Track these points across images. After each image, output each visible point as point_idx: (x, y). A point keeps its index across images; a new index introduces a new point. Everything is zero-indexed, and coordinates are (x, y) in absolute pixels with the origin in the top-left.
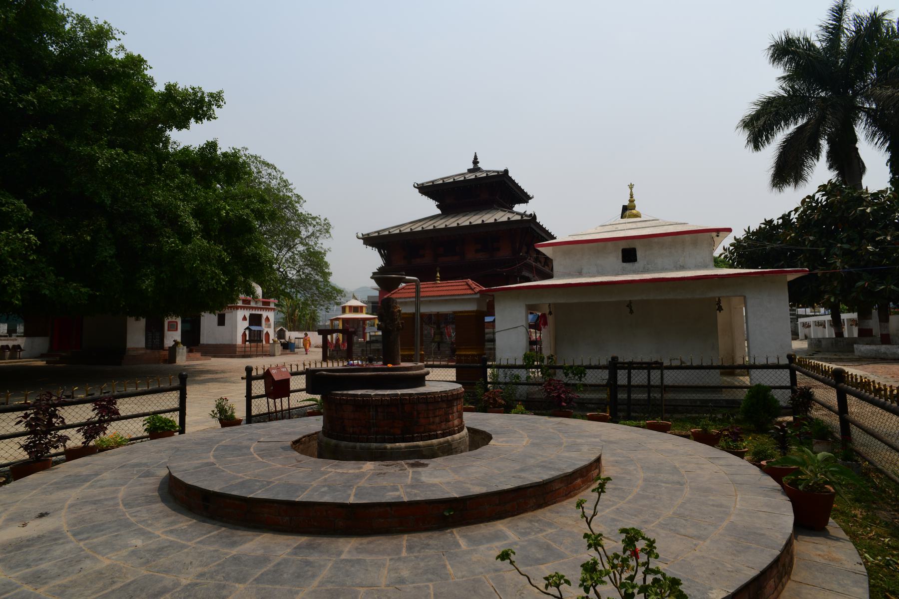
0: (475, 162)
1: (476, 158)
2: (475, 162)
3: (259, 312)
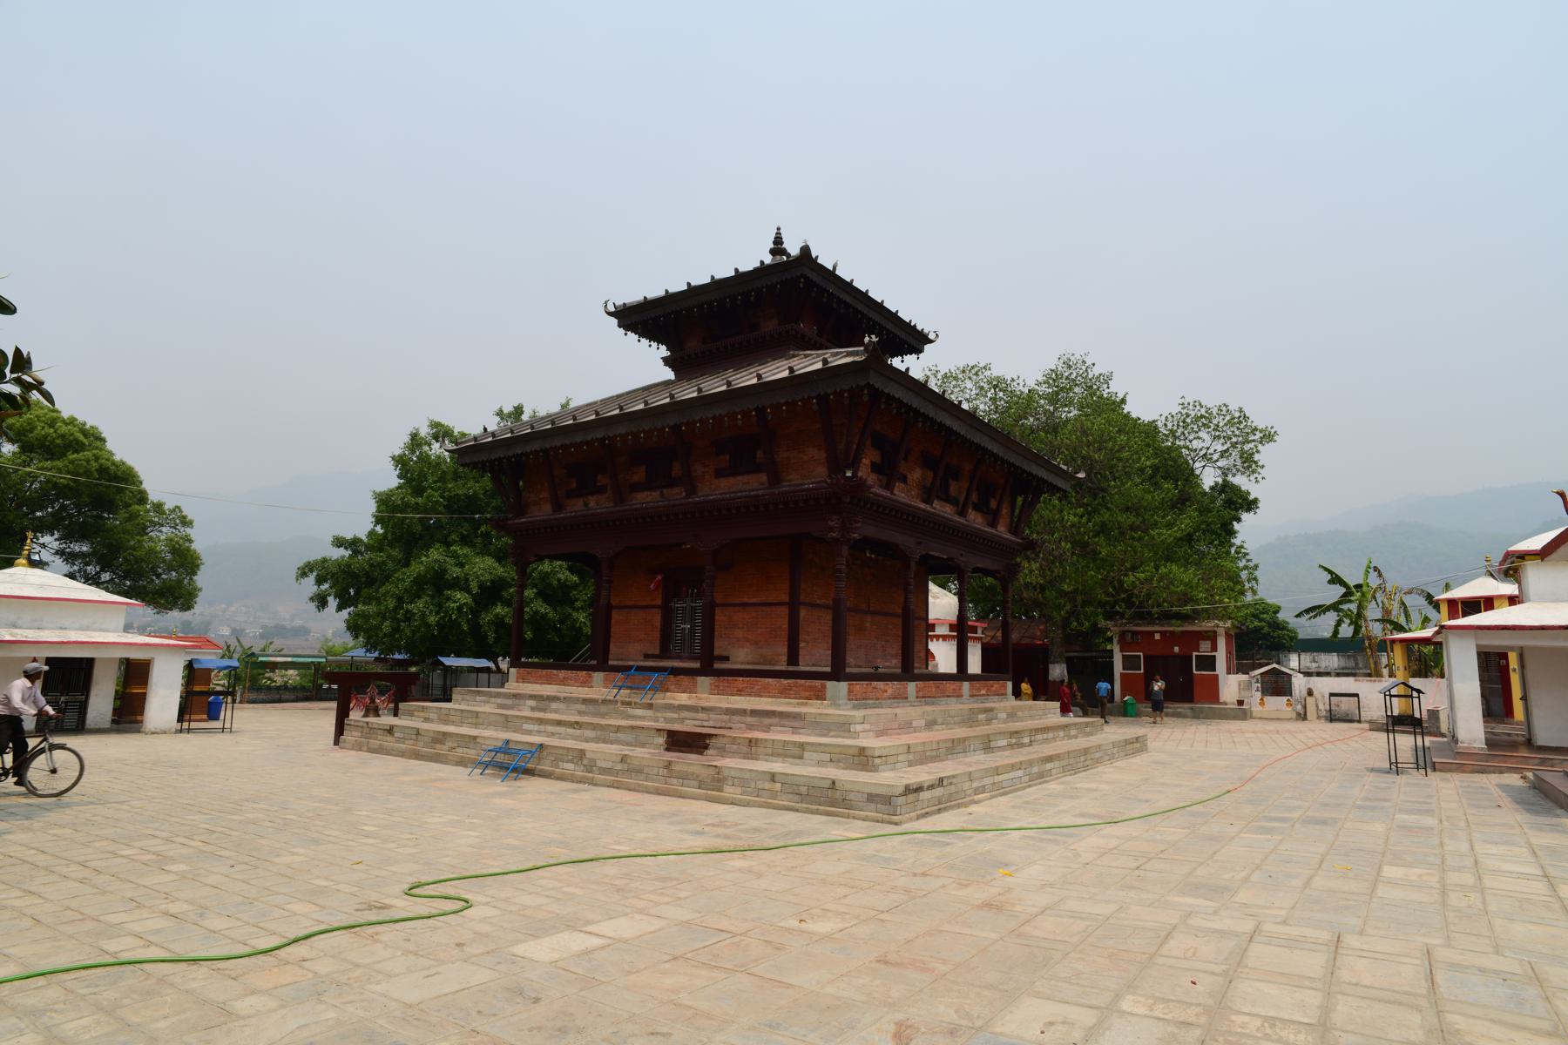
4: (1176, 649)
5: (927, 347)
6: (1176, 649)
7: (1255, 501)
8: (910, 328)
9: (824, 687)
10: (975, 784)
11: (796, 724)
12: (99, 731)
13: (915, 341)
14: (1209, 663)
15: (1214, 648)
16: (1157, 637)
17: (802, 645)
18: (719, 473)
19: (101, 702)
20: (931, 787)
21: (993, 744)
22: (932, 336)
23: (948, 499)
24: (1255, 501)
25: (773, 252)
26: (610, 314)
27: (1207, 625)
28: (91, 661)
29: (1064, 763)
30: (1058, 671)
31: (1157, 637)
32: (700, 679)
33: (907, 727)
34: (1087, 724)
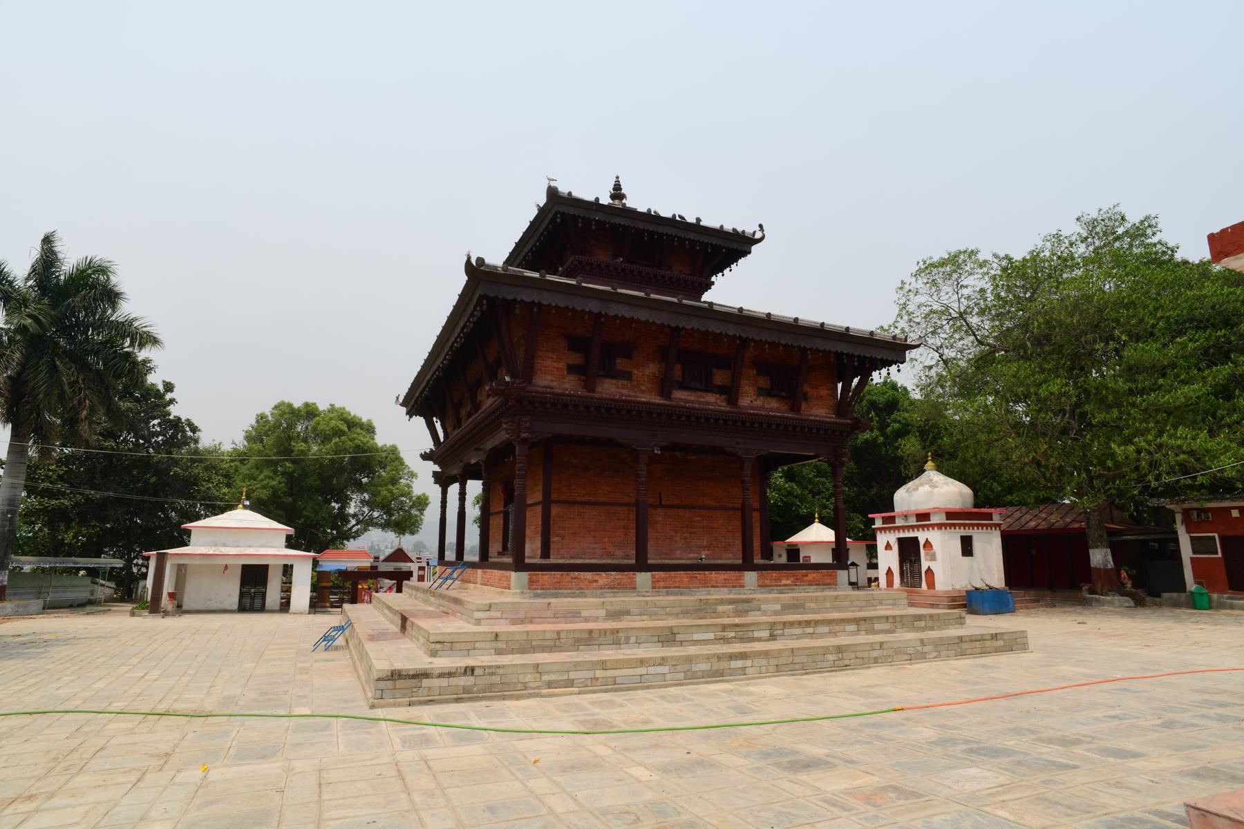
0: (617, 193)
1: (617, 187)
2: (617, 193)
3: (911, 534)
5: (754, 248)
8: (719, 233)
10: (546, 678)
12: (272, 611)
13: (730, 247)
16: (1235, 513)
19: (273, 594)
20: (441, 676)
21: (679, 637)
23: (709, 388)
25: (613, 197)
28: (266, 566)
29: (773, 662)
30: (1099, 557)
31: (1235, 513)
33: (575, 615)
34: (919, 618)
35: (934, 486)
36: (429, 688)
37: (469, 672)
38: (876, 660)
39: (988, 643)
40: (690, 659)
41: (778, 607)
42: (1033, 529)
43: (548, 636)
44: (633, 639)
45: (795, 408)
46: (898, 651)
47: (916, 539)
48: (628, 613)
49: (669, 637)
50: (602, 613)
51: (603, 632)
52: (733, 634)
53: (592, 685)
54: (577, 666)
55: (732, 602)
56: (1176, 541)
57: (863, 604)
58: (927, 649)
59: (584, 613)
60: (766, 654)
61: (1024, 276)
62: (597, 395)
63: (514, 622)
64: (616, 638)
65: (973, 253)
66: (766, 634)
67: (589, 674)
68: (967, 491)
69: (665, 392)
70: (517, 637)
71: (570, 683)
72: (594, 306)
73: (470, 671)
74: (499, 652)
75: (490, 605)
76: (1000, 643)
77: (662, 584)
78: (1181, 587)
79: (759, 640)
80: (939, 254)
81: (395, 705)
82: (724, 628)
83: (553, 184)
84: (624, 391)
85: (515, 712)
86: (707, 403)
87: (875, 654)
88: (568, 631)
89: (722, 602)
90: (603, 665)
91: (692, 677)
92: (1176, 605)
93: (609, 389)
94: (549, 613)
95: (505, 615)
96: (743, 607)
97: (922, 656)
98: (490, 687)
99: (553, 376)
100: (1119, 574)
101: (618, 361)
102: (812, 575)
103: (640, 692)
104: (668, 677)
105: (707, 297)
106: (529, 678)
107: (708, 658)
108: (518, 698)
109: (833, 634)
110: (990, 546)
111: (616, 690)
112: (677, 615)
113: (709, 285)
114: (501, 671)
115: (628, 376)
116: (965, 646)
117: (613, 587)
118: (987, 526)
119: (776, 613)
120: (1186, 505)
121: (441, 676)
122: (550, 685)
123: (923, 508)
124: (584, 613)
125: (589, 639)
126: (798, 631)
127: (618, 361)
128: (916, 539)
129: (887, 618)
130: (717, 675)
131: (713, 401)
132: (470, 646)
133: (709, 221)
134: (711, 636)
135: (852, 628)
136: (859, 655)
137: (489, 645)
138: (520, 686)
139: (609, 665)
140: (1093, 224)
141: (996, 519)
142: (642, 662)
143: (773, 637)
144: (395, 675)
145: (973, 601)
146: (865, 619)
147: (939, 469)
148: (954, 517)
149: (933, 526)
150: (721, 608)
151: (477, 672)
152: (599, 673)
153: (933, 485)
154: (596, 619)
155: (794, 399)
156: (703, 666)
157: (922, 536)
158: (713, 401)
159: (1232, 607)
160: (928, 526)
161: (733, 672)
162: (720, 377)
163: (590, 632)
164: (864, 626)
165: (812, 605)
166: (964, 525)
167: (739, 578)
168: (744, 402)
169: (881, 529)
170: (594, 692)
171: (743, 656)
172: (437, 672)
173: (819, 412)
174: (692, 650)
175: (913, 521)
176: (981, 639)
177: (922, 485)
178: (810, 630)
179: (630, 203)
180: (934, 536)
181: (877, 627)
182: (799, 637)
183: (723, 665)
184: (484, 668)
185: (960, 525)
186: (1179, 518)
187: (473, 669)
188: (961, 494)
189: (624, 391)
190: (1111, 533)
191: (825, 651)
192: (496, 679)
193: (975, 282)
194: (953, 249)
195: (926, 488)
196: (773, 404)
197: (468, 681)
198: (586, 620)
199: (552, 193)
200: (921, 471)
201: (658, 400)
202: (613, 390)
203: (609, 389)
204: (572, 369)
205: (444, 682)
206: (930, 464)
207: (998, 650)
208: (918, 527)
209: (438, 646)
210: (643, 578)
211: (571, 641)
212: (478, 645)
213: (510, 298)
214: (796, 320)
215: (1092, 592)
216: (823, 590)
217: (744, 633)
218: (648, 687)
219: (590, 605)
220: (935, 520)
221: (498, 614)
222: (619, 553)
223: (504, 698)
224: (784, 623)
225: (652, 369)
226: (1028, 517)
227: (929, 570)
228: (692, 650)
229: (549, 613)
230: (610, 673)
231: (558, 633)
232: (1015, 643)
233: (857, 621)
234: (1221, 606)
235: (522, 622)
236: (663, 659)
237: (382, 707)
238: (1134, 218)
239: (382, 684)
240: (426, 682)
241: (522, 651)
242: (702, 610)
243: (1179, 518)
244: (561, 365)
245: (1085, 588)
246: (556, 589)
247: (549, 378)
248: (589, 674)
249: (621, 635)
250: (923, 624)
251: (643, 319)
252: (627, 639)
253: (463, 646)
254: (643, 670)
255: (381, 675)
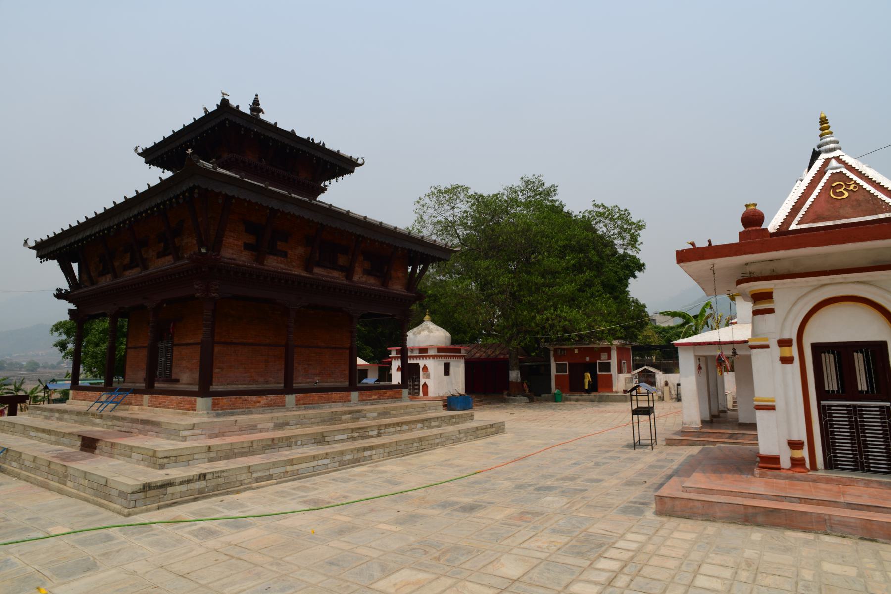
1: (256, 102)
2: (256, 107)
4: (587, 359)
5: (356, 169)
6: (587, 359)
7: (644, 265)
8: (336, 155)
9: (195, 401)
10: (255, 475)
11: (157, 429)
13: (343, 166)
14: (607, 367)
15: (610, 358)
16: (576, 351)
17: (216, 370)
18: (160, 256)
20: (182, 483)
21: (327, 439)
22: (360, 161)
23: (334, 267)
24: (644, 265)
25: (252, 109)
26: (139, 154)
27: (606, 343)
29: (387, 450)
30: (514, 375)
31: (576, 351)
32: (145, 396)
33: (253, 428)
34: (453, 417)
35: (430, 331)
36: (173, 494)
37: (202, 478)
38: (437, 445)
39: (489, 430)
40: (342, 453)
41: (375, 414)
42: (479, 358)
43: (245, 445)
44: (299, 442)
45: (384, 284)
46: (448, 438)
47: (418, 364)
48: (287, 424)
49: (320, 439)
50: (271, 425)
51: (281, 439)
52: (357, 434)
53: (285, 477)
54: (275, 465)
55: (350, 412)
56: (550, 365)
57: (419, 410)
58: (462, 435)
59: (259, 426)
60: (383, 446)
61: (488, 209)
62: (266, 268)
63: (211, 436)
64: (289, 442)
65: (467, 189)
66: (375, 433)
67: (282, 470)
68: (448, 334)
69: (308, 268)
70: (224, 448)
71: (270, 477)
72: (275, 204)
73: (202, 477)
74: (211, 460)
75: (194, 425)
76: (493, 429)
77: (302, 402)
78: (549, 390)
79: (372, 437)
80: (444, 185)
81: (147, 511)
82: (353, 430)
83: (226, 97)
84: (282, 266)
85: (249, 501)
86: (334, 277)
87: (437, 441)
88: (258, 440)
89: (344, 413)
90: (291, 462)
91: (343, 465)
92: (547, 400)
93: (273, 263)
94: (236, 428)
95: (204, 432)
96: (357, 415)
97: (458, 440)
98: (217, 487)
99: (234, 251)
100: (523, 385)
101: (279, 243)
102: (389, 392)
103: (314, 478)
104: (329, 466)
105: (322, 198)
106: (244, 477)
107: (352, 451)
108: (237, 492)
109: (411, 430)
110: (459, 369)
111: (299, 479)
112: (318, 424)
113: (323, 190)
114: (225, 474)
115: (285, 255)
116: (479, 432)
117: (271, 406)
118: (458, 357)
119: (374, 419)
120: (557, 347)
121: (182, 483)
122: (257, 480)
123: (423, 345)
124: (259, 426)
125: (272, 445)
126: (392, 429)
127: (279, 243)
128: (418, 364)
129: (437, 418)
130: (357, 462)
131: (336, 276)
132: (190, 458)
133: (331, 146)
134: (345, 436)
135: (420, 425)
136: (430, 442)
137: (203, 456)
138: (238, 484)
139: (294, 462)
140: (527, 183)
141: (463, 353)
142: (314, 458)
143: (379, 435)
144: (147, 487)
145: (450, 403)
146: (426, 420)
147: (434, 321)
148: (442, 351)
149: (429, 357)
150: (344, 417)
151: (208, 477)
152: (289, 468)
153: (430, 331)
154: (267, 430)
155: (384, 279)
156: (349, 457)
157: (422, 363)
158: (336, 276)
159: (570, 400)
160: (426, 357)
161: (366, 459)
162: (342, 260)
163: (273, 439)
164: (426, 424)
165: (394, 412)
166: (446, 356)
167: (348, 396)
168: (356, 278)
169: (395, 358)
170: (286, 481)
171: (371, 448)
172: (178, 481)
173: (397, 287)
174: (338, 447)
175: (416, 353)
176: (485, 428)
177: (423, 330)
178: (399, 429)
179: (262, 116)
180: (430, 364)
181: (433, 424)
182: (393, 433)
183: (360, 455)
184: (213, 473)
185: (444, 356)
186: (552, 353)
187: (205, 475)
188: (446, 337)
189: (282, 266)
190: (521, 361)
191: (413, 441)
192: (221, 480)
193: (462, 207)
194: (454, 183)
195: (425, 333)
196: (372, 280)
197: (202, 484)
198: (261, 431)
199: (225, 102)
200: (420, 322)
201: (305, 274)
202: (274, 264)
203: (273, 263)
204: (247, 247)
205: (184, 488)
206: (427, 317)
207: (493, 433)
208: (419, 357)
209: (166, 461)
210: (290, 399)
211: (260, 447)
212: (196, 457)
213: (217, 190)
214: (349, 212)
215: (509, 395)
216: (395, 402)
217: (363, 433)
218: (318, 474)
219: (260, 421)
220: (431, 353)
221: (200, 431)
222: (261, 380)
223: (227, 493)
224: (386, 425)
225: (300, 251)
226: (475, 350)
227: (425, 385)
228: (338, 447)
229: (236, 428)
230: (295, 467)
231: (252, 442)
232: (497, 429)
233: (423, 421)
234: (567, 400)
235: (216, 436)
236: (327, 454)
237: (136, 514)
238: (547, 185)
239: (135, 496)
240: (170, 490)
241: (227, 457)
242: (334, 419)
243: (552, 353)
244: (239, 243)
245: (506, 393)
246: (231, 410)
247: (231, 252)
248: (282, 470)
249: (292, 440)
250: (454, 420)
251: (306, 217)
252: (296, 442)
253: (185, 459)
254: (314, 463)
255: (134, 489)
